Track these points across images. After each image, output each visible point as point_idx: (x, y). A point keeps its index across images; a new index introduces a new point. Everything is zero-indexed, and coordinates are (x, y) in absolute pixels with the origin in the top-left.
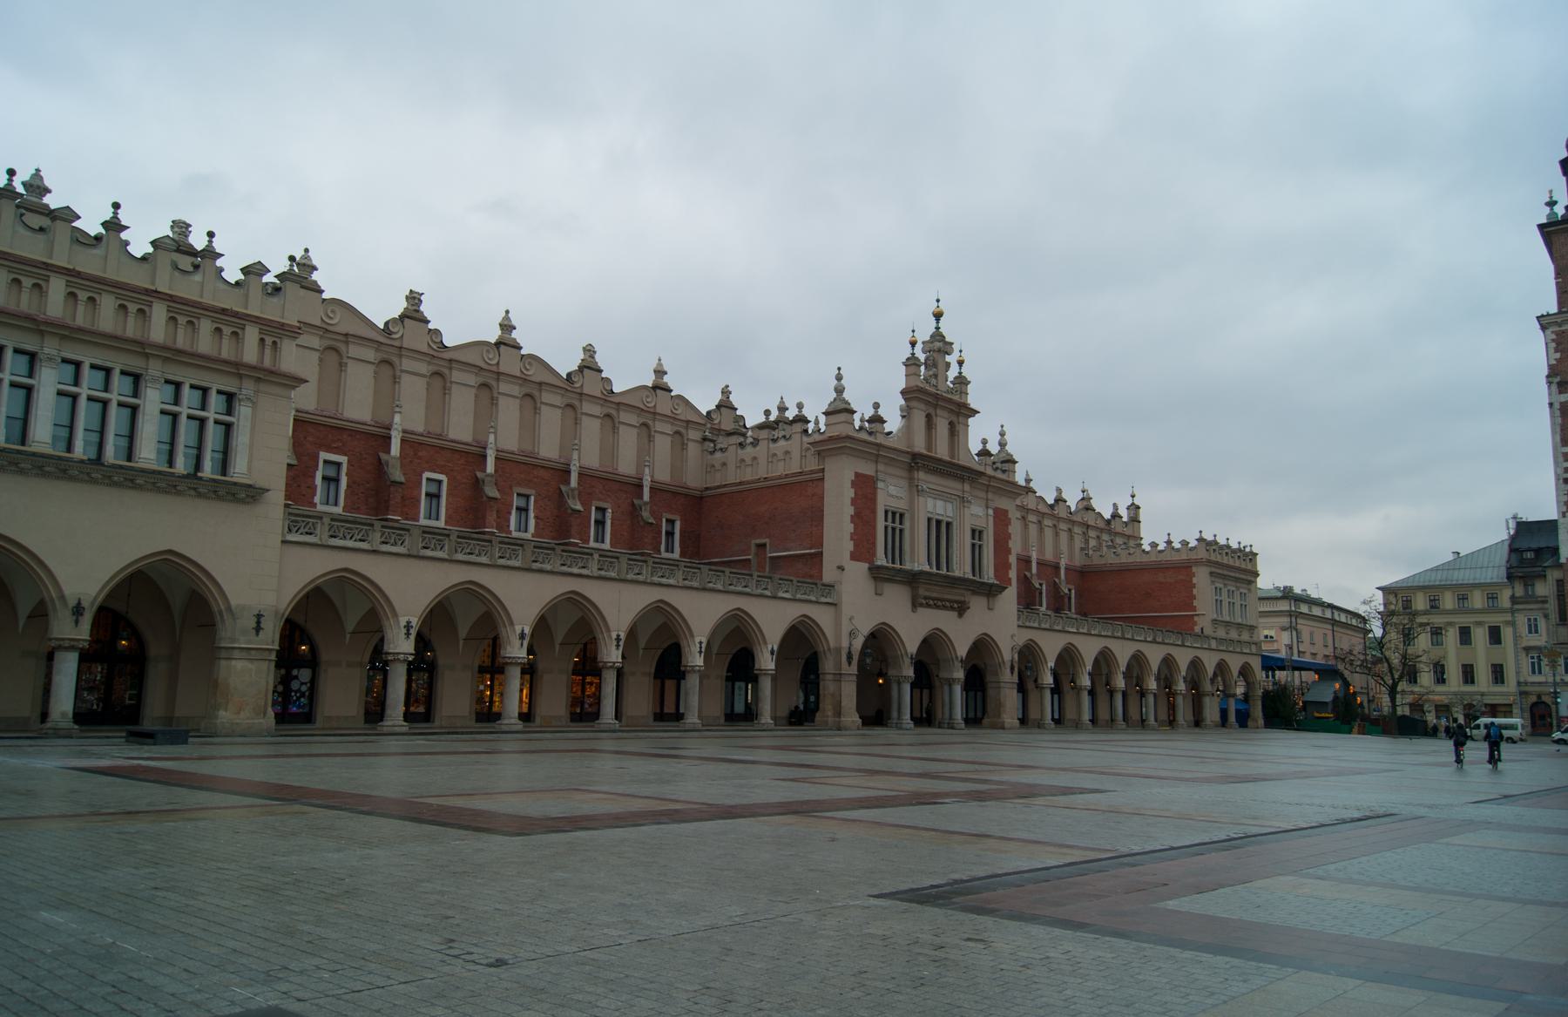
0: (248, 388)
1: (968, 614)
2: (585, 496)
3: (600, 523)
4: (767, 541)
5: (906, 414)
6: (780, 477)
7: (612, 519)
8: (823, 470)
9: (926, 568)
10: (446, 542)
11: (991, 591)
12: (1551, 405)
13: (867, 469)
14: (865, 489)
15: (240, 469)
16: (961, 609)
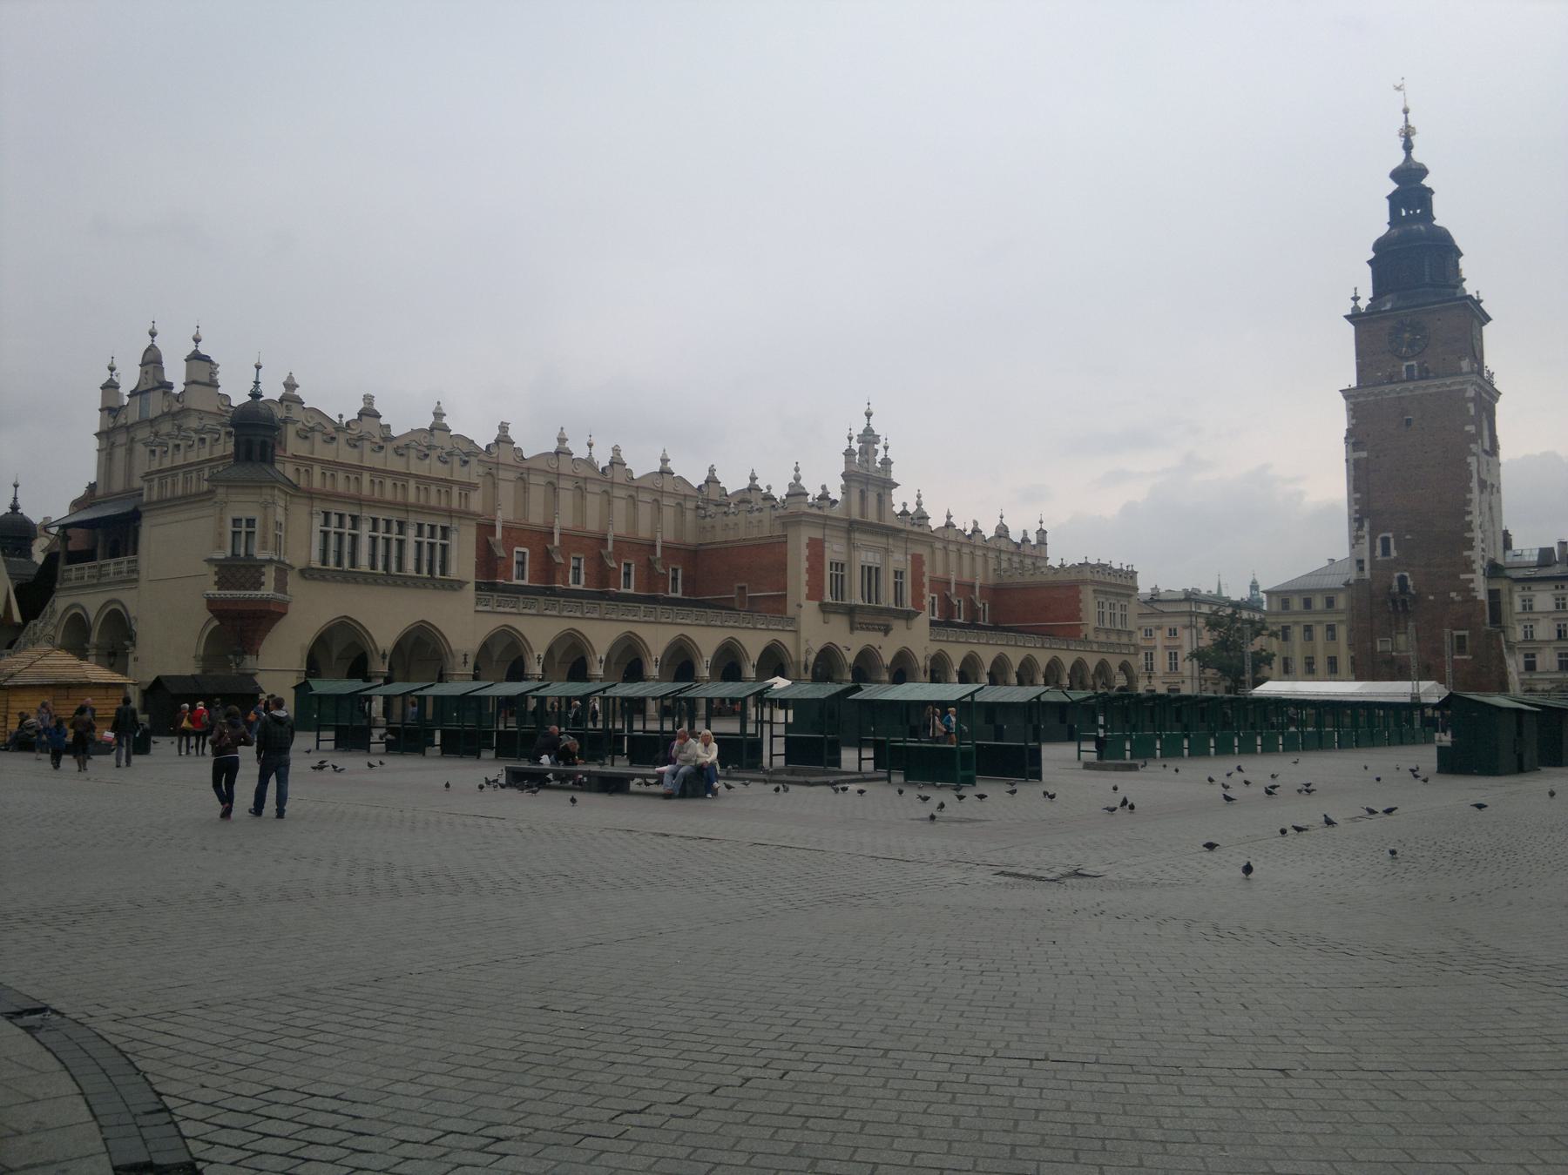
0: (455, 523)
1: (891, 632)
2: (618, 555)
3: (627, 574)
4: (746, 584)
5: (846, 490)
6: (755, 539)
7: (635, 571)
8: (786, 536)
9: (860, 602)
10: (557, 605)
11: (908, 616)
12: (1347, 460)
13: (817, 534)
14: (816, 547)
15: (454, 572)
16: (887, 630)
